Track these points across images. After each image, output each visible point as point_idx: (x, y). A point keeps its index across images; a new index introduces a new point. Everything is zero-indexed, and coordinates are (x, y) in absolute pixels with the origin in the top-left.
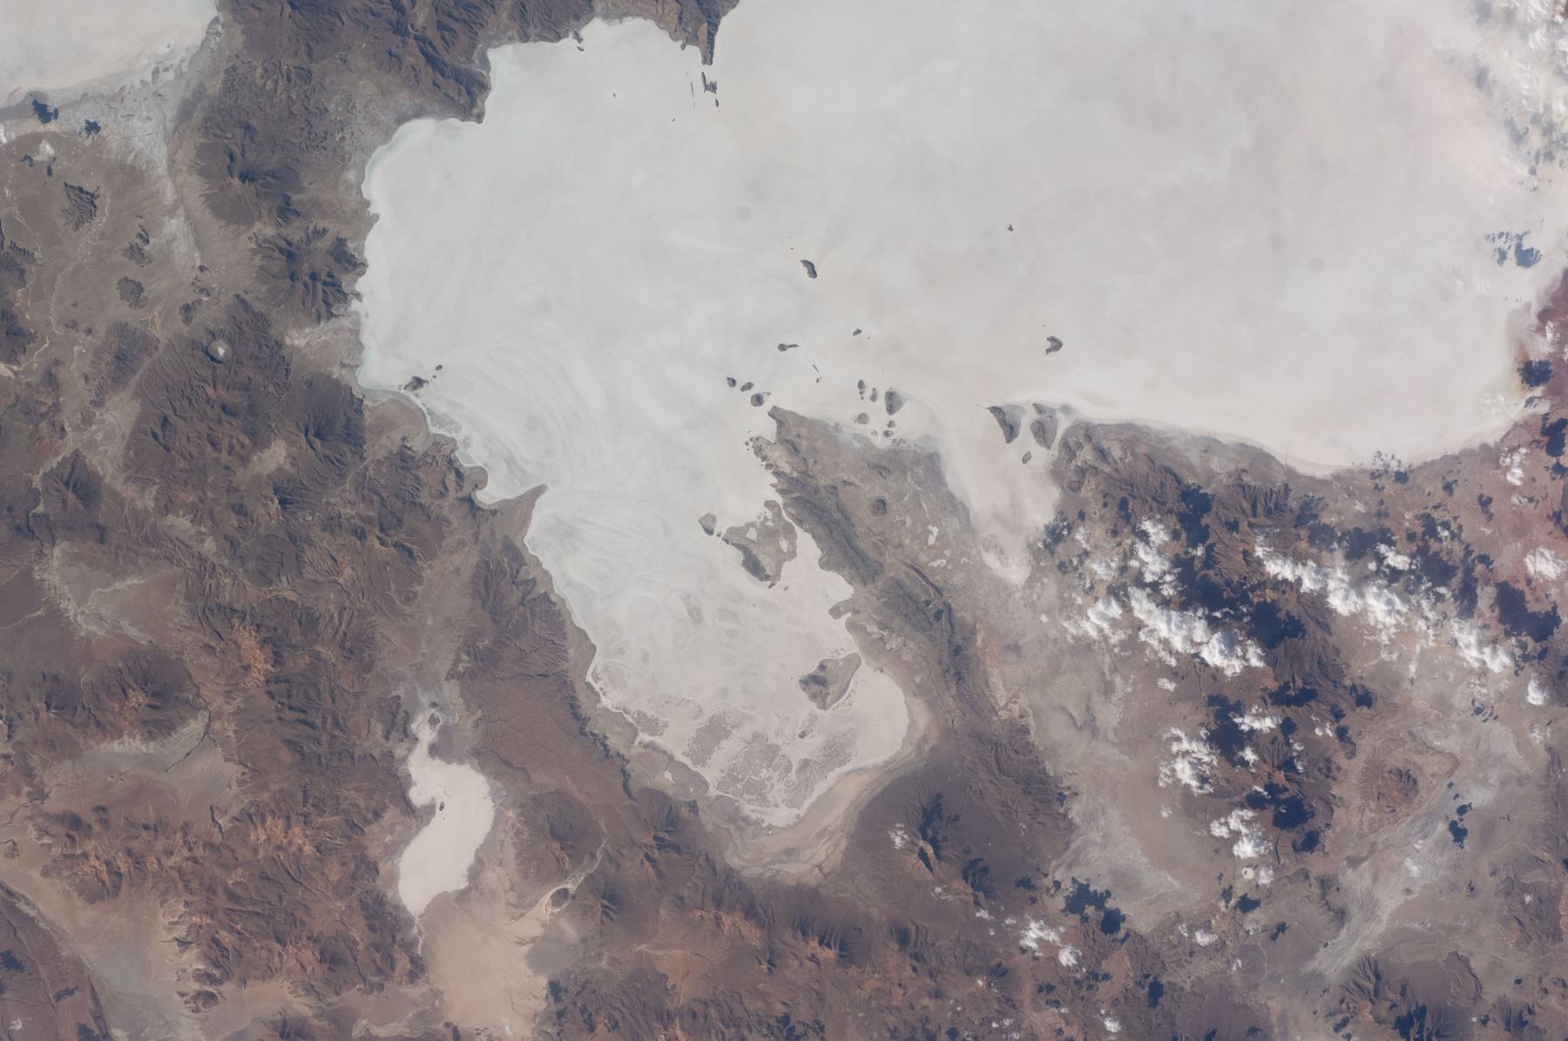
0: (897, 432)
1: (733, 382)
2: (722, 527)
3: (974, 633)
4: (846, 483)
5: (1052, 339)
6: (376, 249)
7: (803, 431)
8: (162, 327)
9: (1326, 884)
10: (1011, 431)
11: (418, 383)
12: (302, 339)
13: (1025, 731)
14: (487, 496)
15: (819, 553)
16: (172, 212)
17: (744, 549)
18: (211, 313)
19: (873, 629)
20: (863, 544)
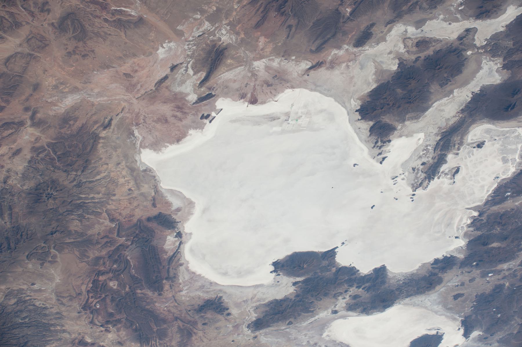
0: (401, 172)
1: (413, 201)
2: (452, 181)
3: (443, 132)
4: (422, 172)
5: (354, 166)
6: (430, 259)
7: (415, 185)
8: (476, 272)
9: (460, 38)
10: (384, 159)
11: (456, 237)
12: (461, 256)
13: (462, 110)
14: (476, 214)
15: (444, 165)
16: (448, 286)
17: (454, 176)
18: (466, 269)
19: (456, 147)
20: (436, 161)
